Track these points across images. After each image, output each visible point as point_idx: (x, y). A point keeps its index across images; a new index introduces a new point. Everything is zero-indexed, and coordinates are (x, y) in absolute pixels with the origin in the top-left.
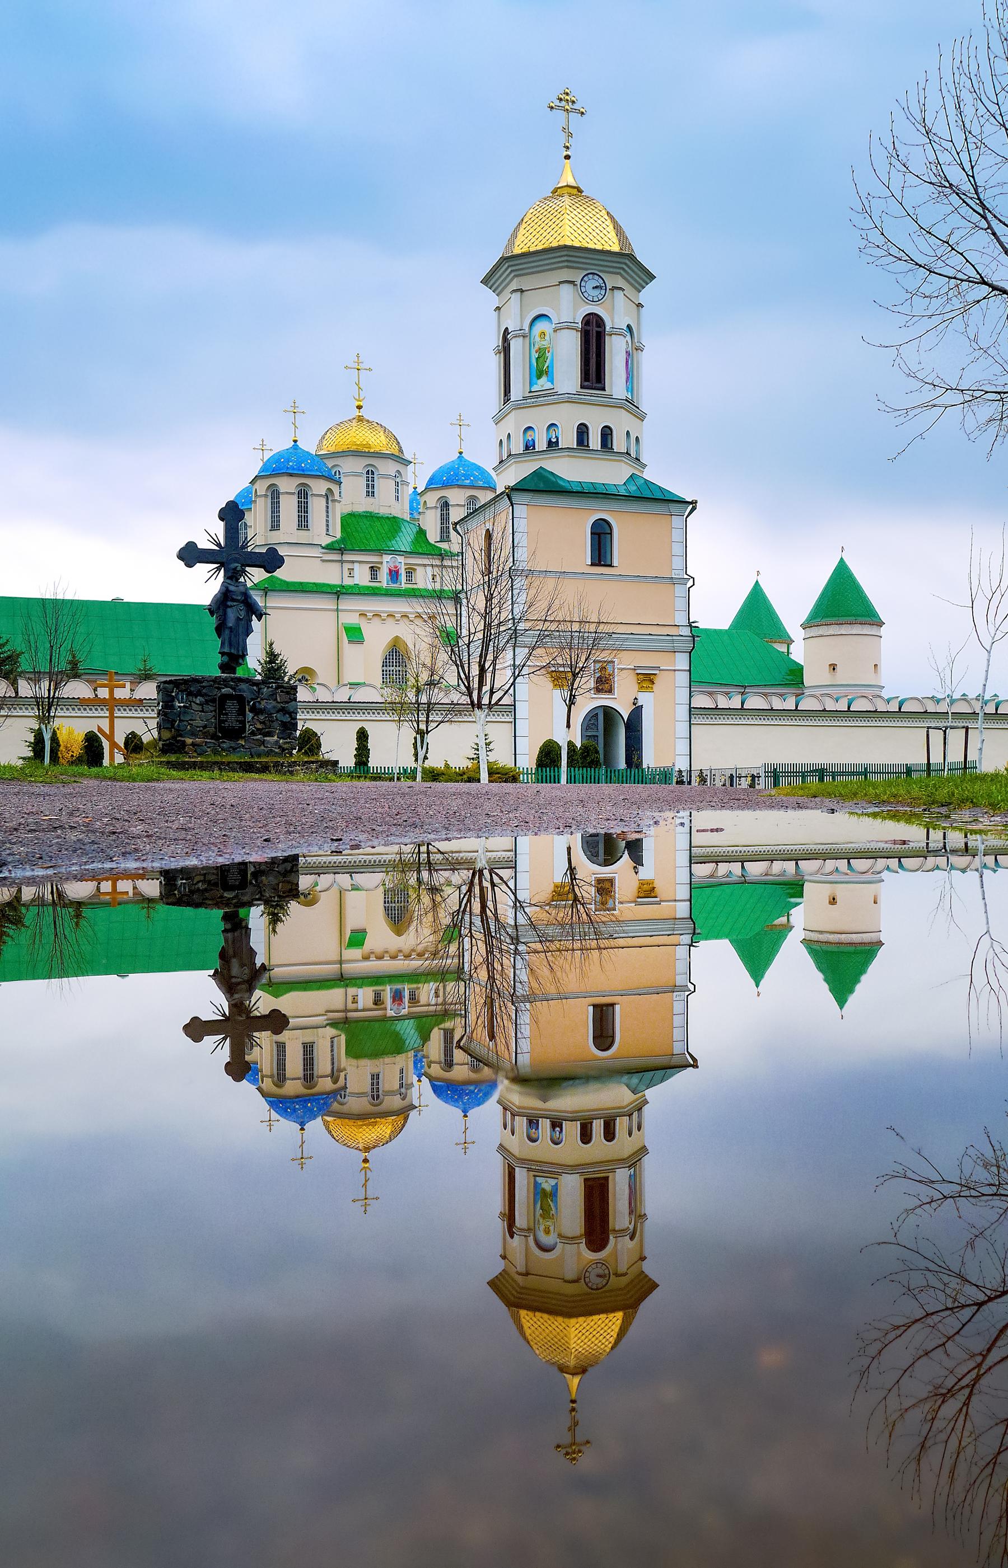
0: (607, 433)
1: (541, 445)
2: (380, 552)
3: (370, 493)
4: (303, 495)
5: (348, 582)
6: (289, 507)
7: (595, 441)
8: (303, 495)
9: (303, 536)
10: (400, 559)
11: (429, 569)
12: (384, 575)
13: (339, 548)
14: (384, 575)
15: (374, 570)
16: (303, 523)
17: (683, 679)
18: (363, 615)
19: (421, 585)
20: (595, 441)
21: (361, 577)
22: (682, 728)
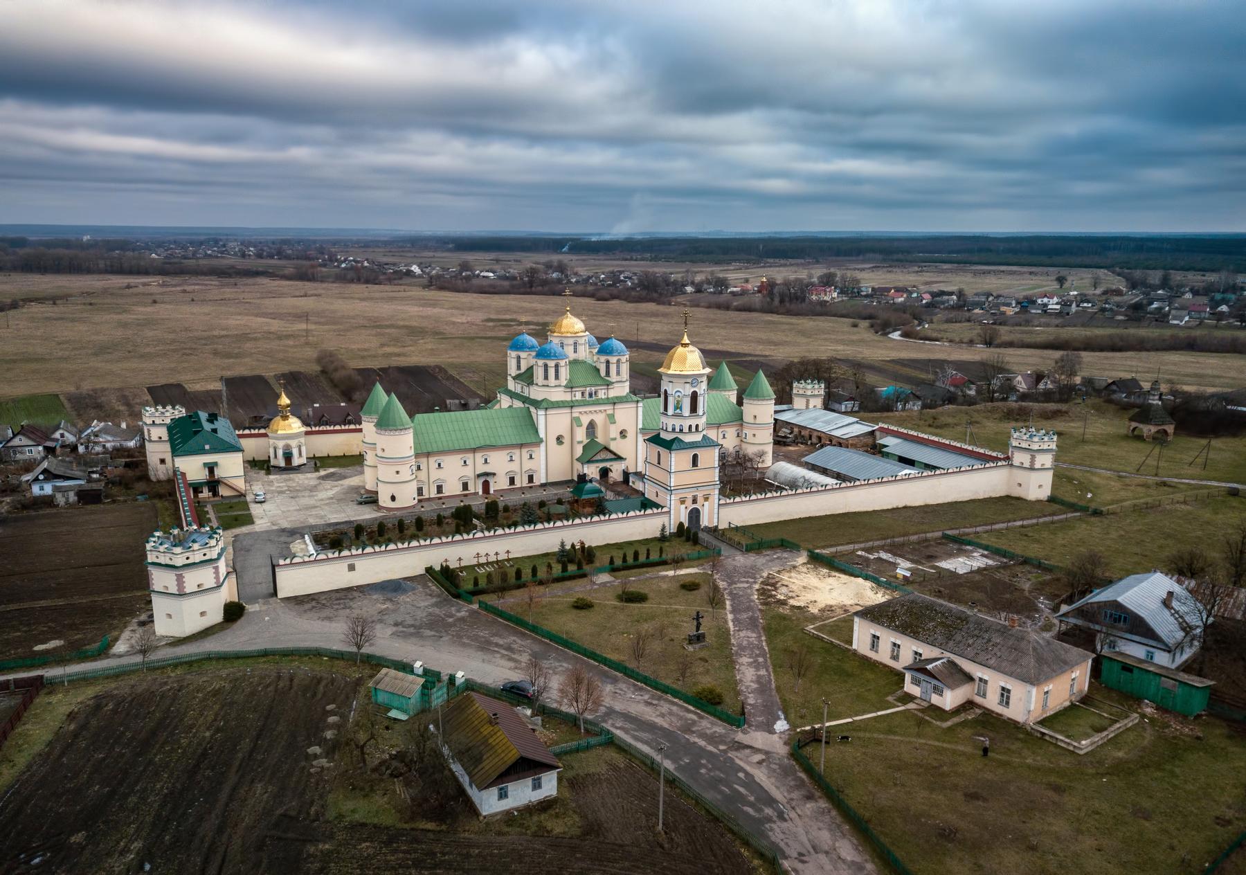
0: (697, 426)
1: (678, 430)
2: (585, 386)
3: (575, 351)
4: (557, 366)
5: (574, 399)
6: (552, 372)
7: (694, 429)
8: (557, 366)
9: (557, 383)
10: (593, 389)
11: (603, 391)
12: (587, 395)
13: (570, 387)
14: (587, 395)
15: (583, 394)
16: (557, 377)
17: (717, 496)
18: (580, 413)
19: (600, 397)
20: (694, 429)
21: (578, 396)
22: (716, 510)
